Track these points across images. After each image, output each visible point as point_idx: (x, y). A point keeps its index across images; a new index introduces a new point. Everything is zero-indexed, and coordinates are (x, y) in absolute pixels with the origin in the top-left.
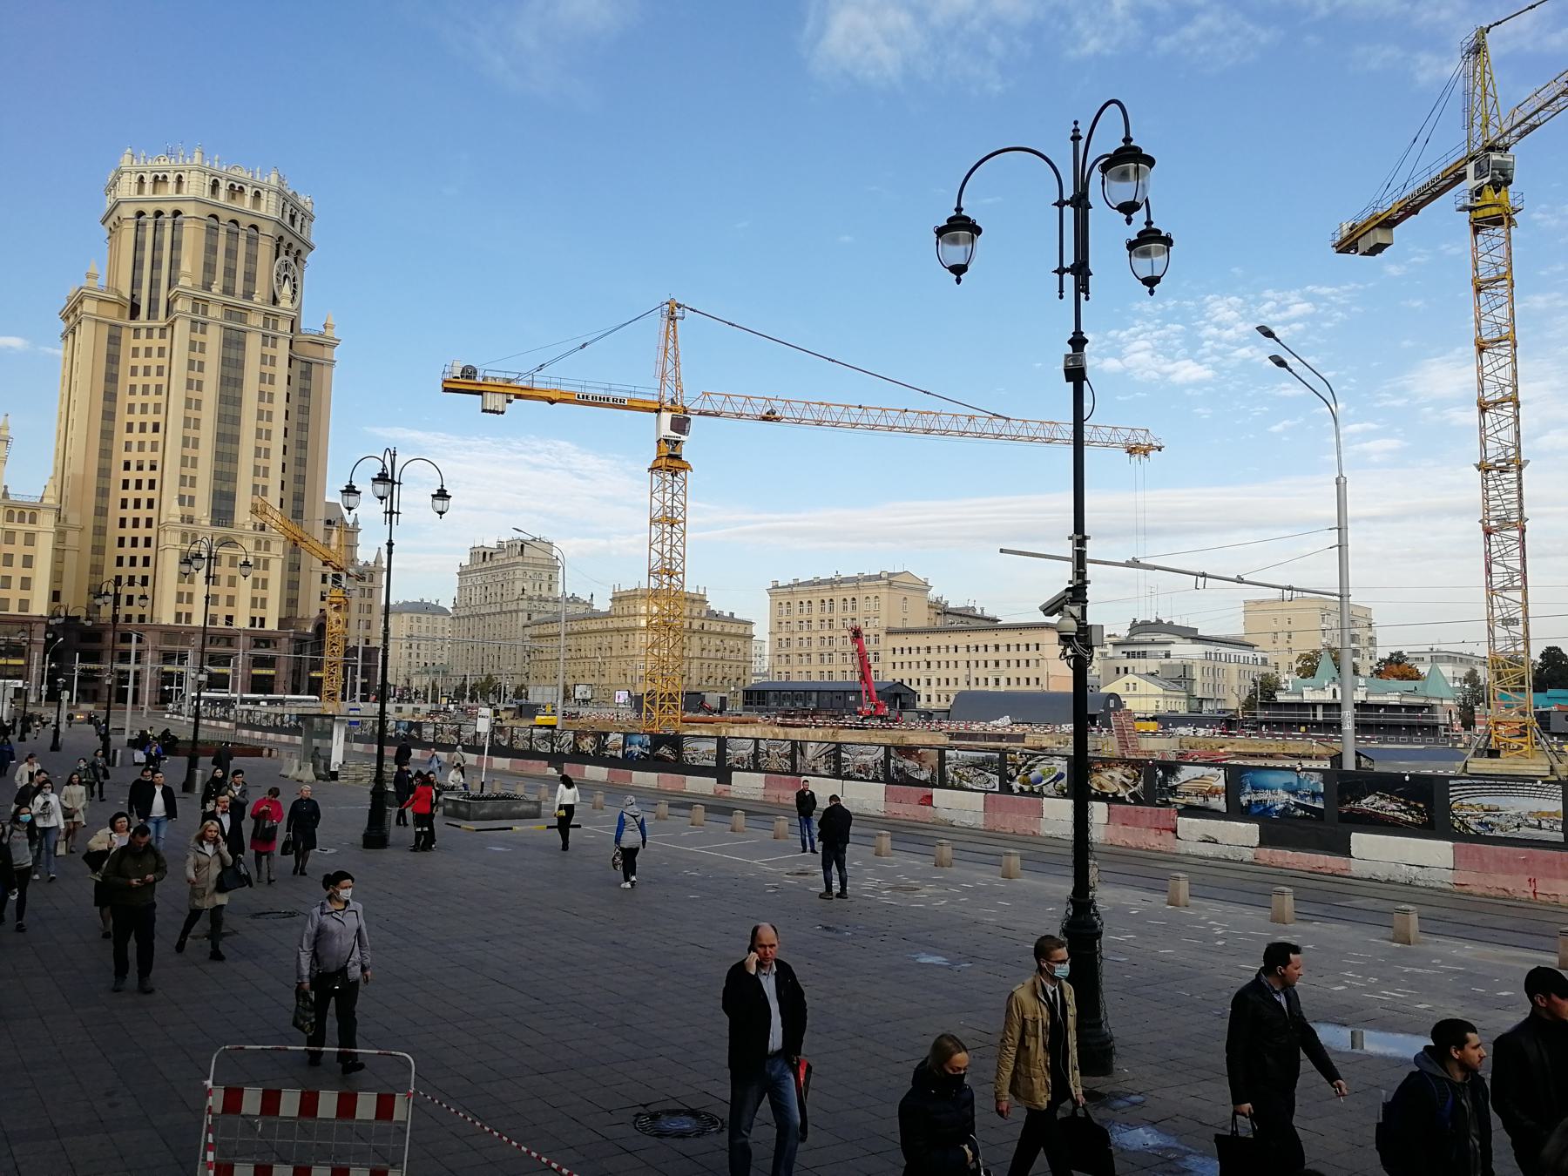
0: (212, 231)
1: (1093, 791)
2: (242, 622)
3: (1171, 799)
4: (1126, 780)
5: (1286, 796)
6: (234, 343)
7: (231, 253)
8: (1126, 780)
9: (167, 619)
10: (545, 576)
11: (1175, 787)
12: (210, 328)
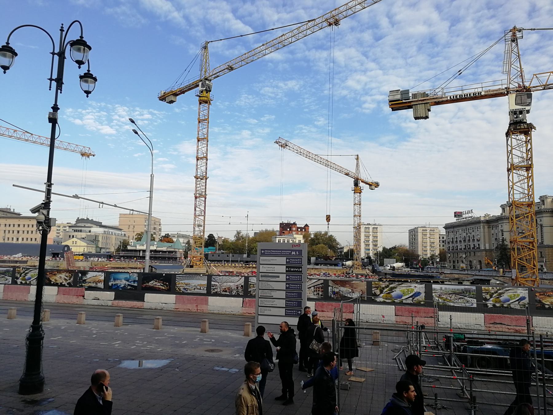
1: (52, 283)
3: (83, 284)
4: (66, 278)
5: (125, 282)
8: (66, 278)
11: (85, 280)
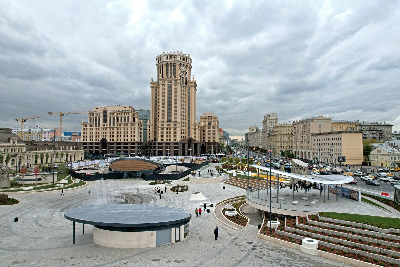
0: (167, 66)
2: (172, 140)
6: (170, 87)
7: (171, 70)
9: (160, 141)
10: (275, 122)
12: (165, 85)
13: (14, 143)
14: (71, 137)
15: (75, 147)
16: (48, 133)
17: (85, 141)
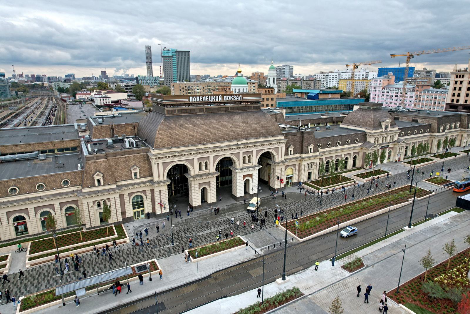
13: (386, 127)
14: (413, 87)
15: (458, 125)
16: (380, 81)
17: (455, 102)
